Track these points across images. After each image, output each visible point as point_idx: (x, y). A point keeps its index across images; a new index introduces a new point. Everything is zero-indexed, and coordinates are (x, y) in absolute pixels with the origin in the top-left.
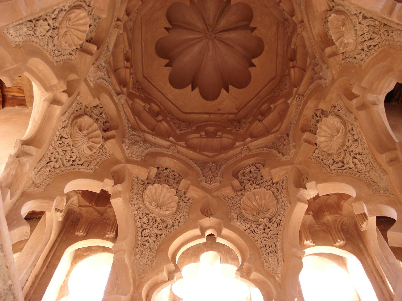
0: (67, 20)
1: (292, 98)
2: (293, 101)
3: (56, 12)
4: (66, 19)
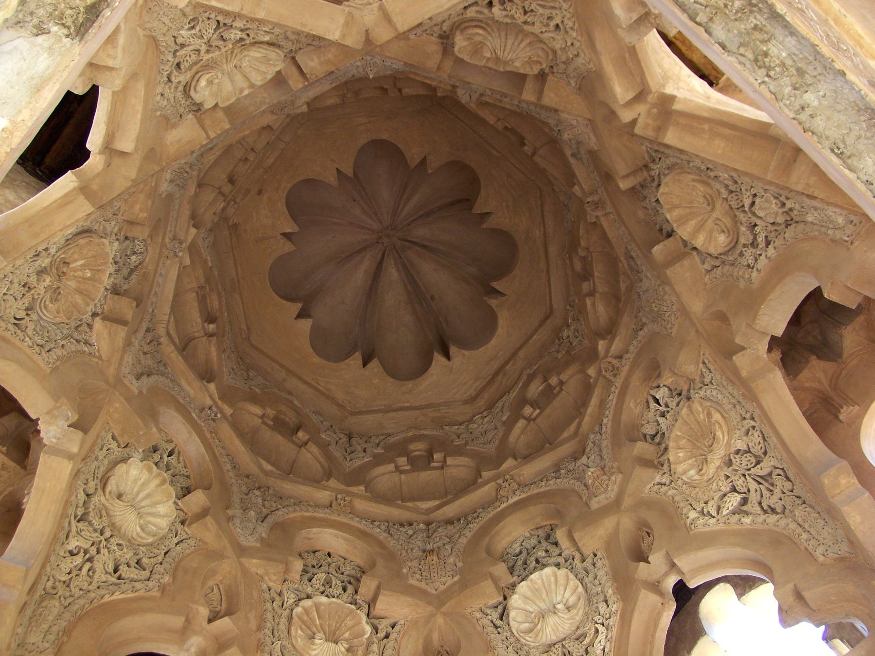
0: (728, 230)
1: (216, 396)
2: (211, 397)
3: (761, 239)
4: (731, 233)
